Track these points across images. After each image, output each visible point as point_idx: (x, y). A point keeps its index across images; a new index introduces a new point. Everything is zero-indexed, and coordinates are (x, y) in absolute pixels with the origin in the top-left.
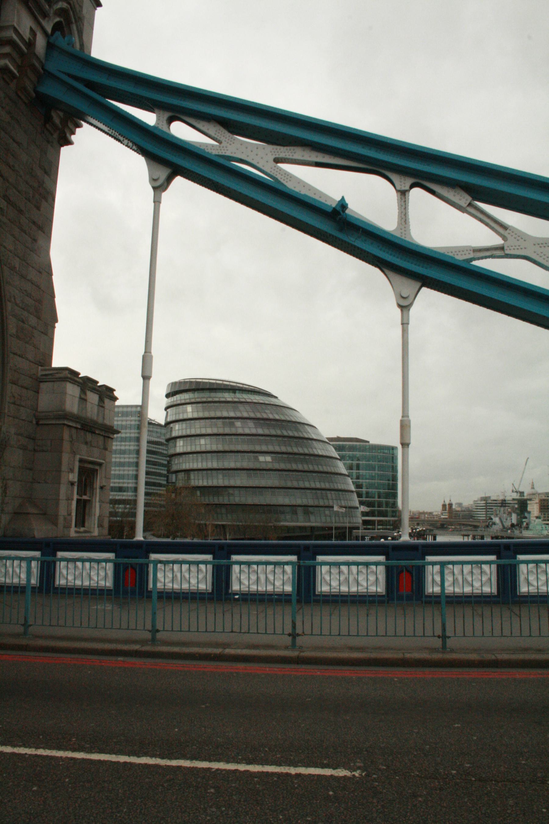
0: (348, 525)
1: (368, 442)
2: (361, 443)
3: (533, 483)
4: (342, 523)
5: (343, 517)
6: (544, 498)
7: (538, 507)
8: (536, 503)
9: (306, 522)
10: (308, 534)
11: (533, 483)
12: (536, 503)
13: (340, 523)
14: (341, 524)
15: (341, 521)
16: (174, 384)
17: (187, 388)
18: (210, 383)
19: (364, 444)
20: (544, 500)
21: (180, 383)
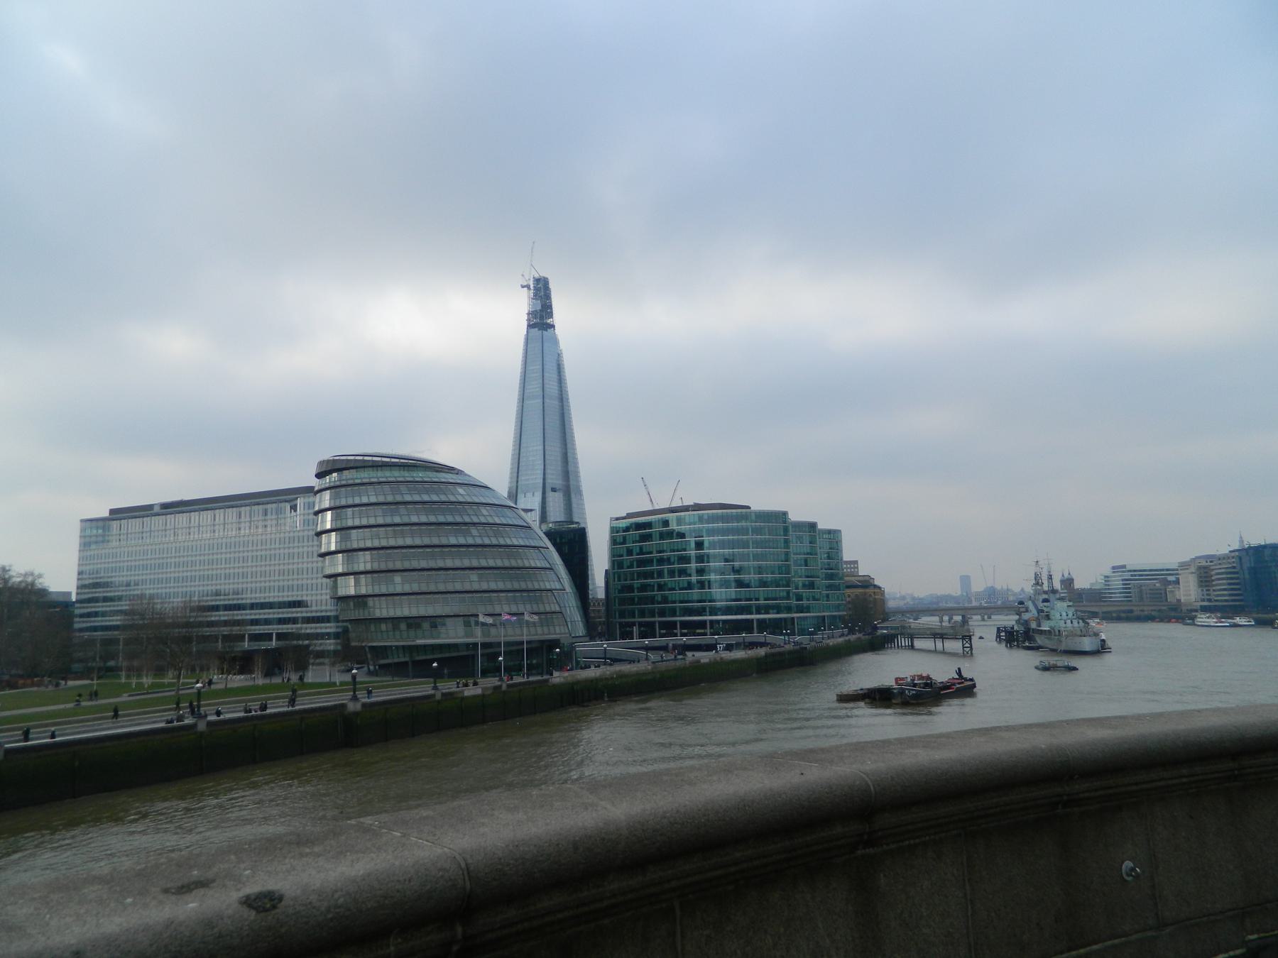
0: (525, 638)
2: (739, 510)
3: (1241, 537)
4: (546, 635)
5: (528, 627)
6: (1204, 564)
7: (1196, 579)
8: (1192, 573)
9: (467, 636)
11: (1241, 537)
12: (1192, 573)
13: (543, 634)
14: (518, 638)
15: (545, 633)
16: (321, 463)
17: (352, 466)
18: (348, 460)
20: (1205, 568)
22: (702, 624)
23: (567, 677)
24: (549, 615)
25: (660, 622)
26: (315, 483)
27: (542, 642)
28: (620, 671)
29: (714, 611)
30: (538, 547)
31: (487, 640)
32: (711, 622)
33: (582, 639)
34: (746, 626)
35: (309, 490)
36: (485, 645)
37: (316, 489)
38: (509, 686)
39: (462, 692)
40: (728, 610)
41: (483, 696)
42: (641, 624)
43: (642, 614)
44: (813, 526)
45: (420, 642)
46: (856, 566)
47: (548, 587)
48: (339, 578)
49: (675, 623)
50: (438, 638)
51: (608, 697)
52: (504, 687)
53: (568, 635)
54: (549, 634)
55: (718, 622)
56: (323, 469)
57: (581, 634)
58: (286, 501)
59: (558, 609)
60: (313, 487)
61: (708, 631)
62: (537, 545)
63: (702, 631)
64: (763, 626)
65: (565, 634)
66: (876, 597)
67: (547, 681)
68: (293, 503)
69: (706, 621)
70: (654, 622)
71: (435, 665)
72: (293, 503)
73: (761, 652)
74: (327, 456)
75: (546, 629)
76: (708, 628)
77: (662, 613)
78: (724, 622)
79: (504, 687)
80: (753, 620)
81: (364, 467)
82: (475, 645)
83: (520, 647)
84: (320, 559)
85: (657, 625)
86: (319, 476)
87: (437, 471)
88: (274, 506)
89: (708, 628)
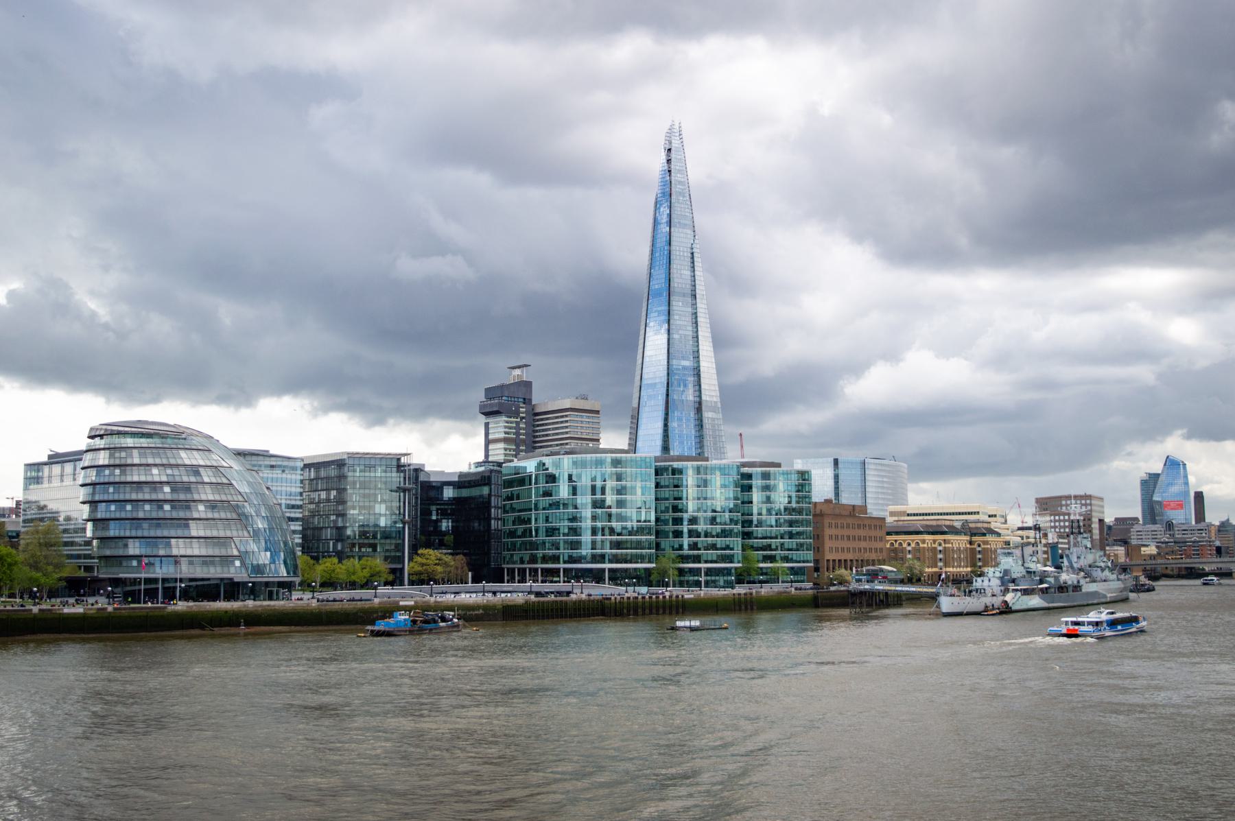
22: (555, 572)
23: (192, 606)
27: (222, 579)
38: (115, 609)
45: (121, 575)
46: (1088, 502)
55: (571, 569)
57: (285, 575)
63: (557, 579)
64: (616, 576)
65: (241, 573)
66: (947, 545)
67: (165, 608)
69: (559, 569)
74: (96, 424)
87: (163, 438)
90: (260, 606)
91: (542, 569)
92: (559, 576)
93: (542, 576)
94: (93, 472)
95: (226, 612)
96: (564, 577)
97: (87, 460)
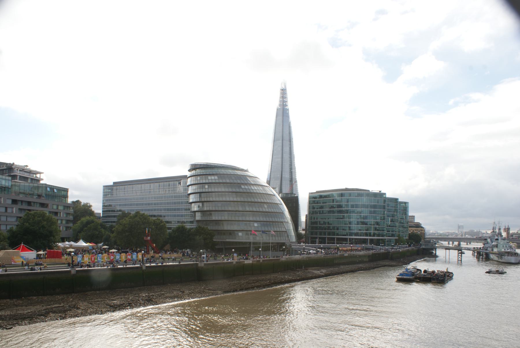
0: (271, 241)
1: (369, 191)
5: (272, 236)
10: (248, 246)
19: (367, 192)
21: (195, 165)
22: (346, 240)
24: (281, 233)
25: (328, 238)
26: (188, 174)
27: (278, 243)
28: (310, 257)
29: (351, 234)
30: (277, 204)
31: (255, 241)
32: (350, 239)
33: (295, 243)
34: (364, 241)
35: (185, 177)
36: (254, 243)
37: (188, 176)
39: (244, 261)
40: (357, 234)
41: (252, 264)
42: (320, 238)
43: (321, 234)
44: (396, 200)
45: (227, 240)
47: (281, 221)
48: (197, 213)
49: (334, 238)
50: (235, 239)
51: (304, 268)
52: (261, 261)
53: (289, 241)
54: (281, 240)
55: (353, 239)
56: (193, 168)
57: (294, 241)
58: (177, 181)
59: (285, 230)
60: (187, 176)
61: (348, 242)
62: (277, 203)
63: (346, 242)
64: (372, 241)
68: (180, 182)
69: (347, 238)
70: (326, 237)
71: (233, 250)
72: (180, 182)
73: (371, 252)
75: (279, 238)
76: (348, 241)
77: (329, 234)
78: (355, 239)
79: (261, 261)
80: (368, 239)
81: (207, 168)
82: (250, 243)
83: (268, 245)
84: (190, 205)
85: (327, 238)
86: (189, 171)
88: (172, 182)
89: (348, 241)
90: (308, 258)
91: (337, 238)
92: (347, 241)
93: (337, 241)
94: (194, 187)
95: (298, 261)
96: (349, 241)
97: (189, 181)
